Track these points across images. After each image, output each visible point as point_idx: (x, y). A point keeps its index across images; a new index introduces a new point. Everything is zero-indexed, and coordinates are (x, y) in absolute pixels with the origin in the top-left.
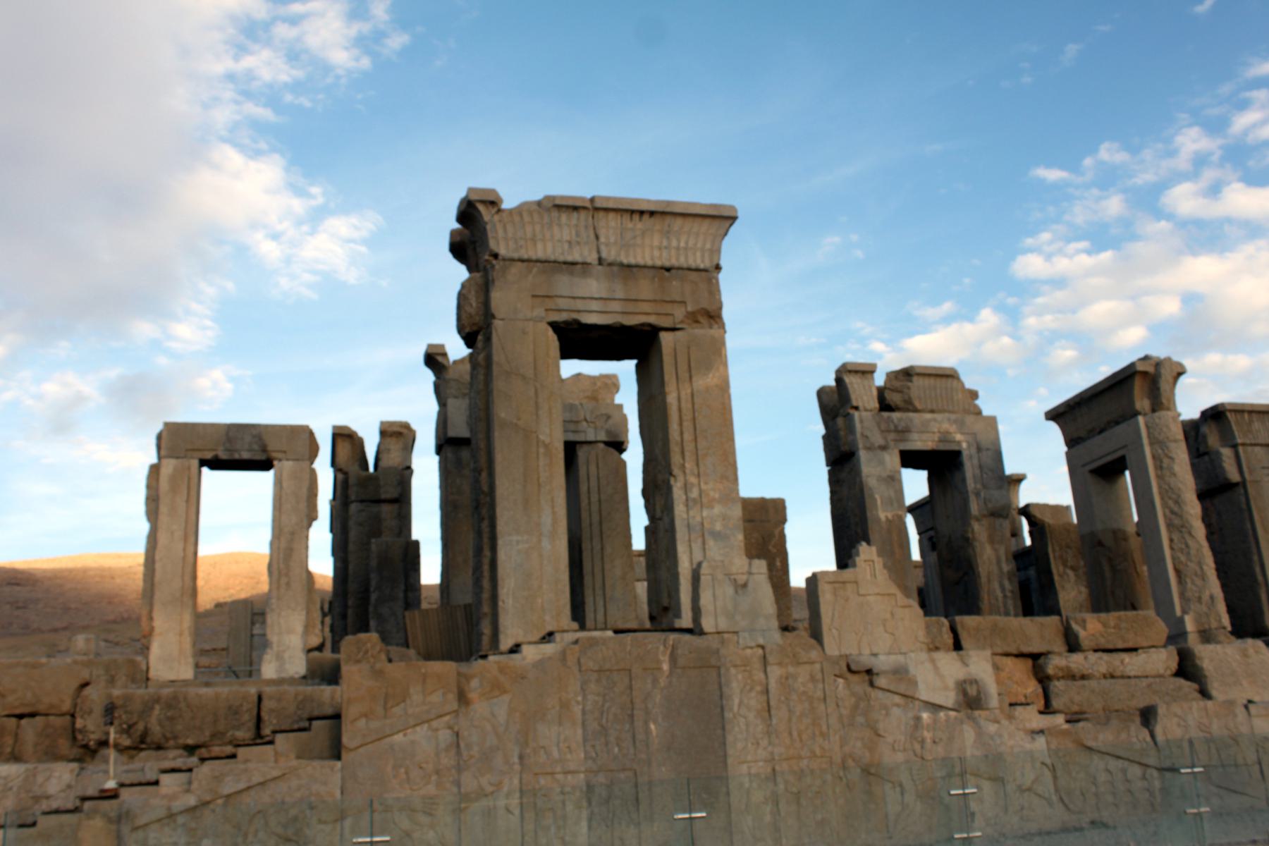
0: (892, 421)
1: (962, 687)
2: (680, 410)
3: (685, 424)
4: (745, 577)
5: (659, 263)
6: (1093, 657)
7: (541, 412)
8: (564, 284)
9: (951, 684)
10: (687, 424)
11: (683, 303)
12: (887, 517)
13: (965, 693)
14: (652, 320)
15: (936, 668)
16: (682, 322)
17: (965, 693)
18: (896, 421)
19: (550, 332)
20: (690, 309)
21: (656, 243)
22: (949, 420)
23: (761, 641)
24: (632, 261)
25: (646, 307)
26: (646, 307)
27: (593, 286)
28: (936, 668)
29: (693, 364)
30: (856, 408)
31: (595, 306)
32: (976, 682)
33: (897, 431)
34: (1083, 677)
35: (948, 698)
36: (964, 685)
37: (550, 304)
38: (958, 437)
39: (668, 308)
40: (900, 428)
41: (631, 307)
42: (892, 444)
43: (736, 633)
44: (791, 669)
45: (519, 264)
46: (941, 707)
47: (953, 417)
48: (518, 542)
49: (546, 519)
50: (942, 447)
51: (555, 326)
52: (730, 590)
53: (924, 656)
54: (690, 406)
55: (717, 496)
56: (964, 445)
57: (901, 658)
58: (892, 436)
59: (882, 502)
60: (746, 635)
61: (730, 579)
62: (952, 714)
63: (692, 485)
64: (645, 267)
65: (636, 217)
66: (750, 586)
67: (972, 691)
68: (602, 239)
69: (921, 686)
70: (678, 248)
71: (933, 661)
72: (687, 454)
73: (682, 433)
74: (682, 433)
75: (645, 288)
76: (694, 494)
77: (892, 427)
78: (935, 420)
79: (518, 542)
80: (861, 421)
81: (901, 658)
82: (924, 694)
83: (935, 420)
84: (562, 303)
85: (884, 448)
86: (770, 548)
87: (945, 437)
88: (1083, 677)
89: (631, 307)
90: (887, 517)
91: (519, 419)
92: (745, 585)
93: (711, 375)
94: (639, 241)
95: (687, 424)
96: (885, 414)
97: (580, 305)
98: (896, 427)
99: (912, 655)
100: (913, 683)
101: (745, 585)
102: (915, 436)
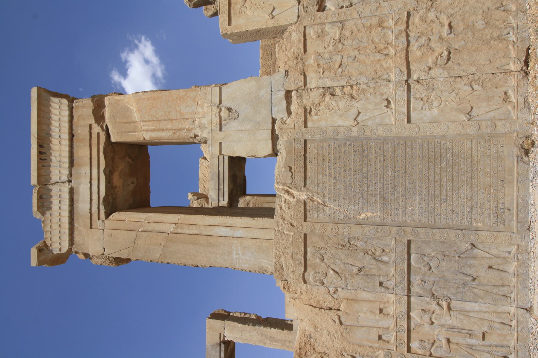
2: (153, 130)
3: (162, 127)
7: (157, 229)
10: (162, 125)
11: (90, 126)
16: (102, 127)
19: (111, 217)
20: (93, 121)
23: (282, 94)
29: (125, 121)
37: (95, 216)
39: (95, 136)
43: (274, 121)
48: (237, 254)
49: (222, 231)
51: (107, 216)
54: (151, 123)
60: (275, 109)
63: (200, 123)
66: (229, 106)
72: (180, 126)
73: (168, 130)
74: (168, 130)
79: (237, 254)
91: (161, 244)
92: (230, 110)
93: (131, 107)
95: (162, 125)
97: (95, 197)
101: (230, 110)
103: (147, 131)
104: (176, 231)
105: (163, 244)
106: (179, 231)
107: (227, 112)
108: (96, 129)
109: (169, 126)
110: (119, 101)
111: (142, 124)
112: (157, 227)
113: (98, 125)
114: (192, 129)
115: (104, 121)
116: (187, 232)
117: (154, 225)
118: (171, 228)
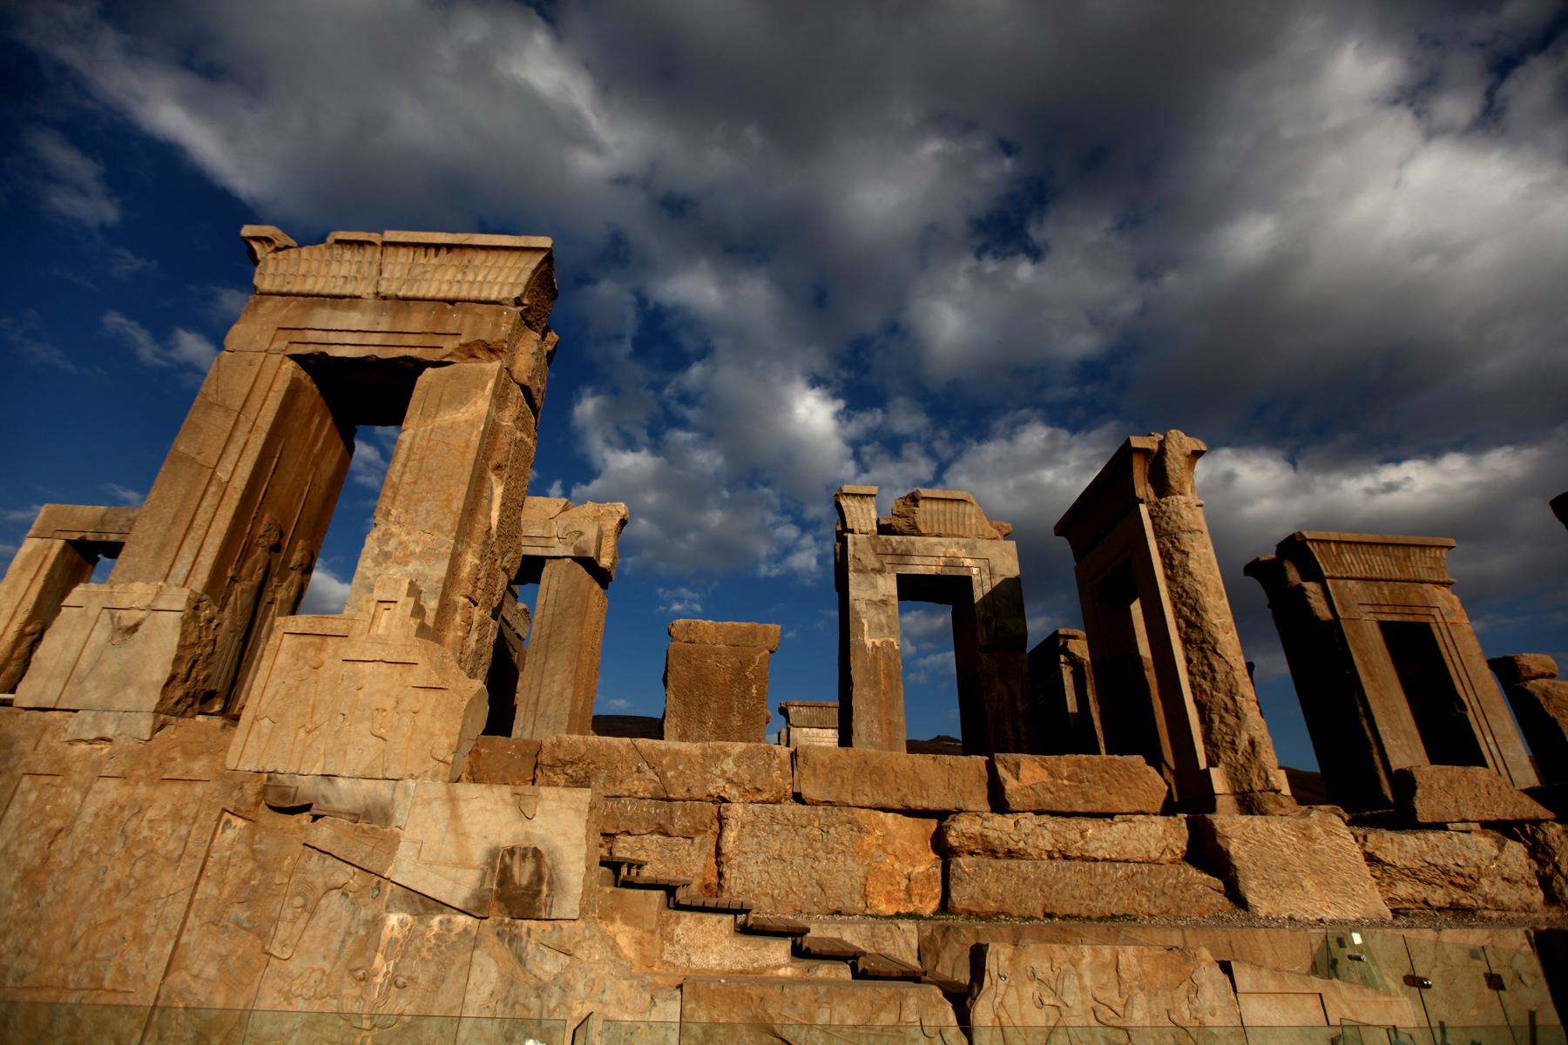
0: (891, 545)
1: (501, 863)
3: (411, 463)
4: (141, 614)
5: (441, 295)
6: (1028, 822)
8: (322, 317)
9: (478, 854)
12: (873, 643)
13: (505, 876)
14: (415, 353)
15: (455, 816)
17: (505, 876)
18: (894, 544)
20: (463, 340)
21: (448, 277)
22: (958, 543)
23: (109, 731)
24: (410, 294)
25: (411, 340)
26: (411, 340)
27: (355, 319)
28: (455, 816)
30: (852, 531)
31: (349, 338)
32: (537, 854)
33: (894, 554)
34: (1010, 854)
35: (458, 885)
36: (507, 859)
37: (297, 336)
38: (968, 562)
39: (438, 341)
40: (899, 551)
41: (393, 340)
42: (888, 567)
44: (142, 790)
45: (279, 297)
46: (441, 905)
47: (962, 541)
50: (947, 572)
52: (101, 634)
53: (438, 788)
55: (418, 550)
56: (975, 571)
57: (383, 789)
58: (889, 559)
59: (869, 626)
61: (112, 617)
62: (461, 920)
63: (392, 535)
64: (424, 299)
65: (432, 252)
67: (522, 874)
68: (386, 275)
69: (404, 851)
70: (472, 283)
71: (452, 800)
72: (400, 498)
75: (417, 320)
76: (393, 543)
77: (890, 550)
78: (941, 544)
80: (855, 544)
81: (383, 789)
82: (405, 869)
83: (941, 544)
84: (311, 336)
85: (880, 571)
86: (747, 673)
87: (952, 562)
88: (1010, 854)
89: (393, 340)
90: (873, 643)
91: (199, 454)
92: (133, 629)
93: (463, 410)
94: (428, 276)
96: (883, 537)
97: (333, 337)
98: (894, 550)
99: (411, 784)
100: (391, 844)
101: (133, 629)
102: (917, 560)
103: (414, 437)
104: (214, 482)
105: (199, 458)
106: (213, 489)
107: (131, 623)
108: (450, 345)
109: (407, 478)
110: (484, 389)
111: (429, 428)
112: (234, 451)
113: (456, 349)
114: (387, 520)
115: (461, 358)
116: (205, 504)
117: (241, 443)
118: (223, 475)
